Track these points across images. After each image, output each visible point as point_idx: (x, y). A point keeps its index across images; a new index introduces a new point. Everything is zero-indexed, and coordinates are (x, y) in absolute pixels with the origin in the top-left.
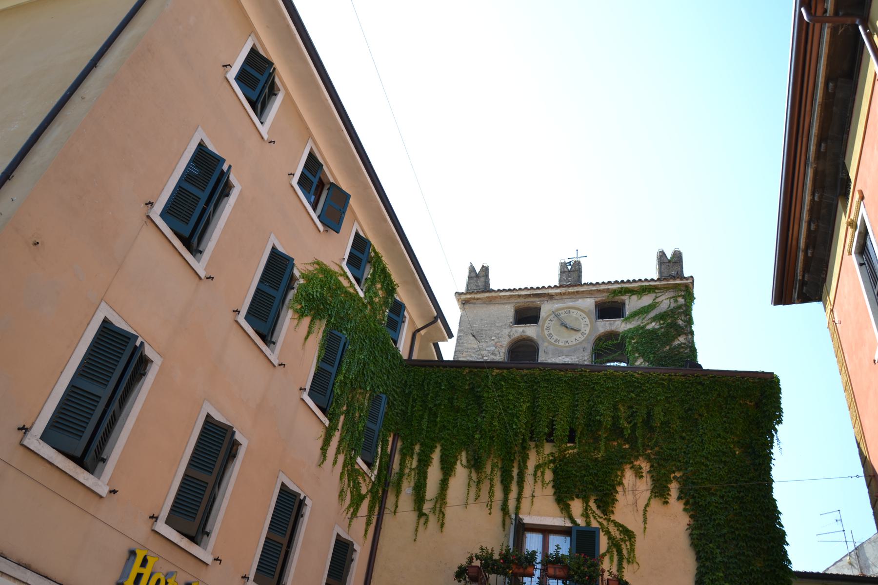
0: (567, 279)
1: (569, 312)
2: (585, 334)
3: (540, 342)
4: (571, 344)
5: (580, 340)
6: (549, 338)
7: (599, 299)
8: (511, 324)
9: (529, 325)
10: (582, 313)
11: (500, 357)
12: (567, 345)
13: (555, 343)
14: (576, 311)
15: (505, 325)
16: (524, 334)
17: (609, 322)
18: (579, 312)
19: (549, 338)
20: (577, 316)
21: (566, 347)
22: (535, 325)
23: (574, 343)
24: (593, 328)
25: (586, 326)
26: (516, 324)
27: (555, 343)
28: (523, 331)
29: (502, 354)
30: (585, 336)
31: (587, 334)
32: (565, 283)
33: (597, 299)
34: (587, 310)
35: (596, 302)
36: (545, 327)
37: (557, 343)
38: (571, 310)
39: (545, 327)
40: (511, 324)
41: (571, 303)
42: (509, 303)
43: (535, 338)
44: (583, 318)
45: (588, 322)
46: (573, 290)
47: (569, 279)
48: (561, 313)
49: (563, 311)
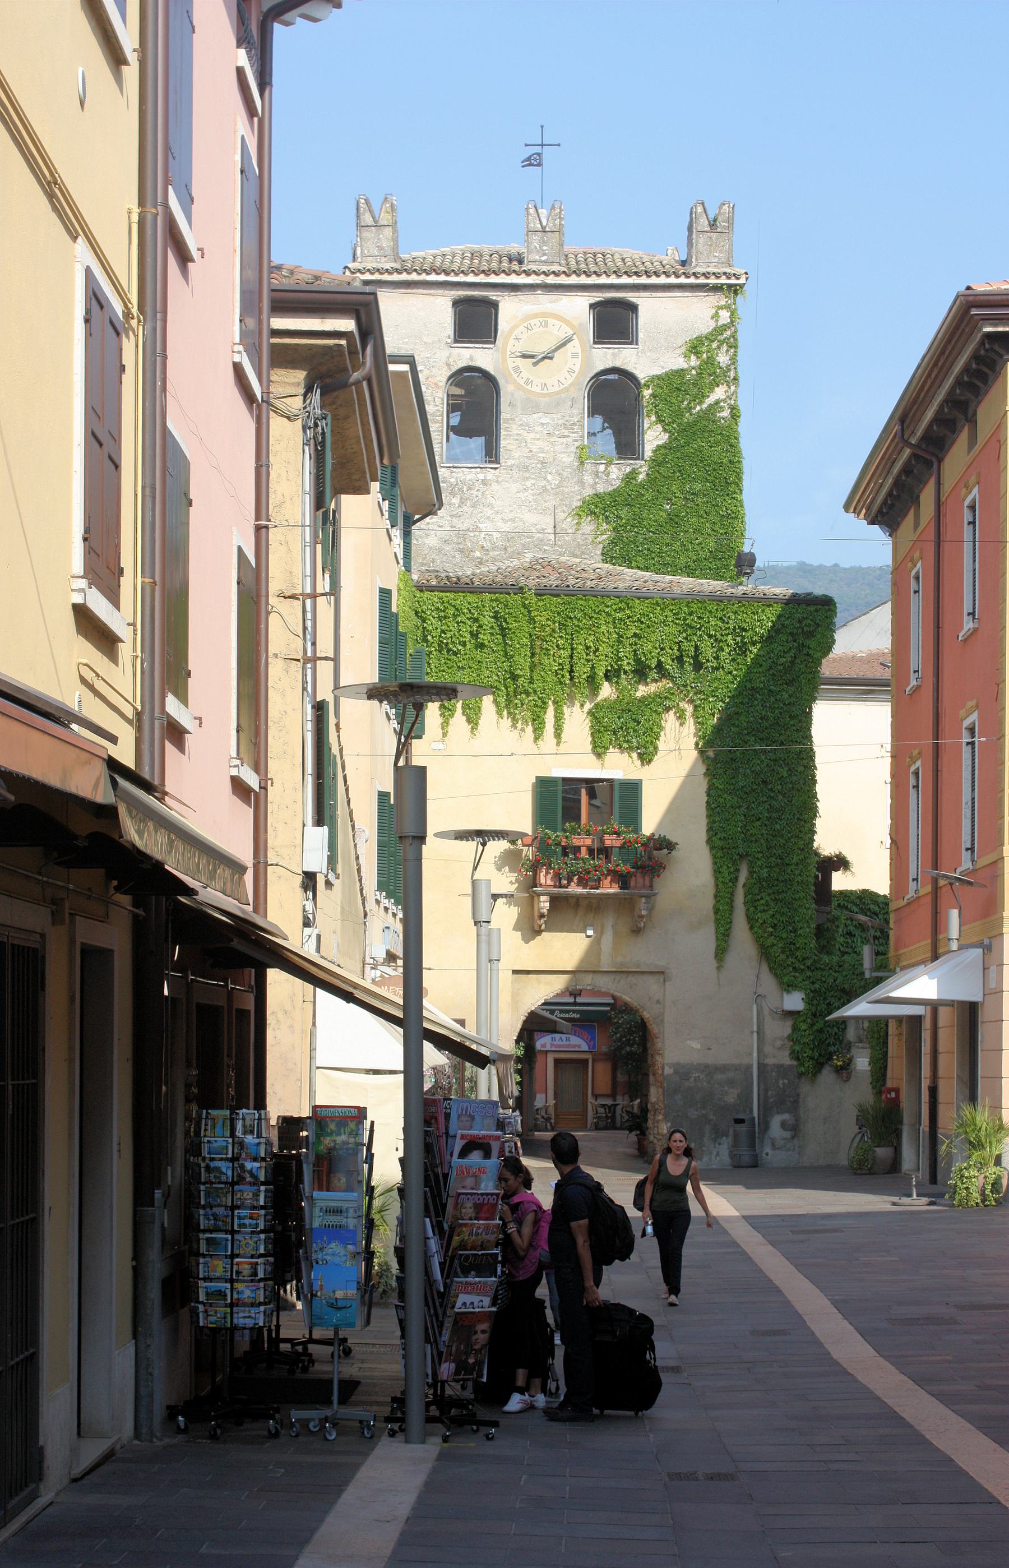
4: (551, 390)
8: (449, 341)
12: (545, 391)
13: (524, 385)
15: (439, 341)
21: (544, 395)
24: (587, 361)
27: (524, 385)
28: (471, 358)
32: (537, 257)
33: (592, 301)
36: (508, 353)
37: (529, 387)
39: (508, 353)
41: (549, 305)
47: (545, 248)
49: (536, 321)
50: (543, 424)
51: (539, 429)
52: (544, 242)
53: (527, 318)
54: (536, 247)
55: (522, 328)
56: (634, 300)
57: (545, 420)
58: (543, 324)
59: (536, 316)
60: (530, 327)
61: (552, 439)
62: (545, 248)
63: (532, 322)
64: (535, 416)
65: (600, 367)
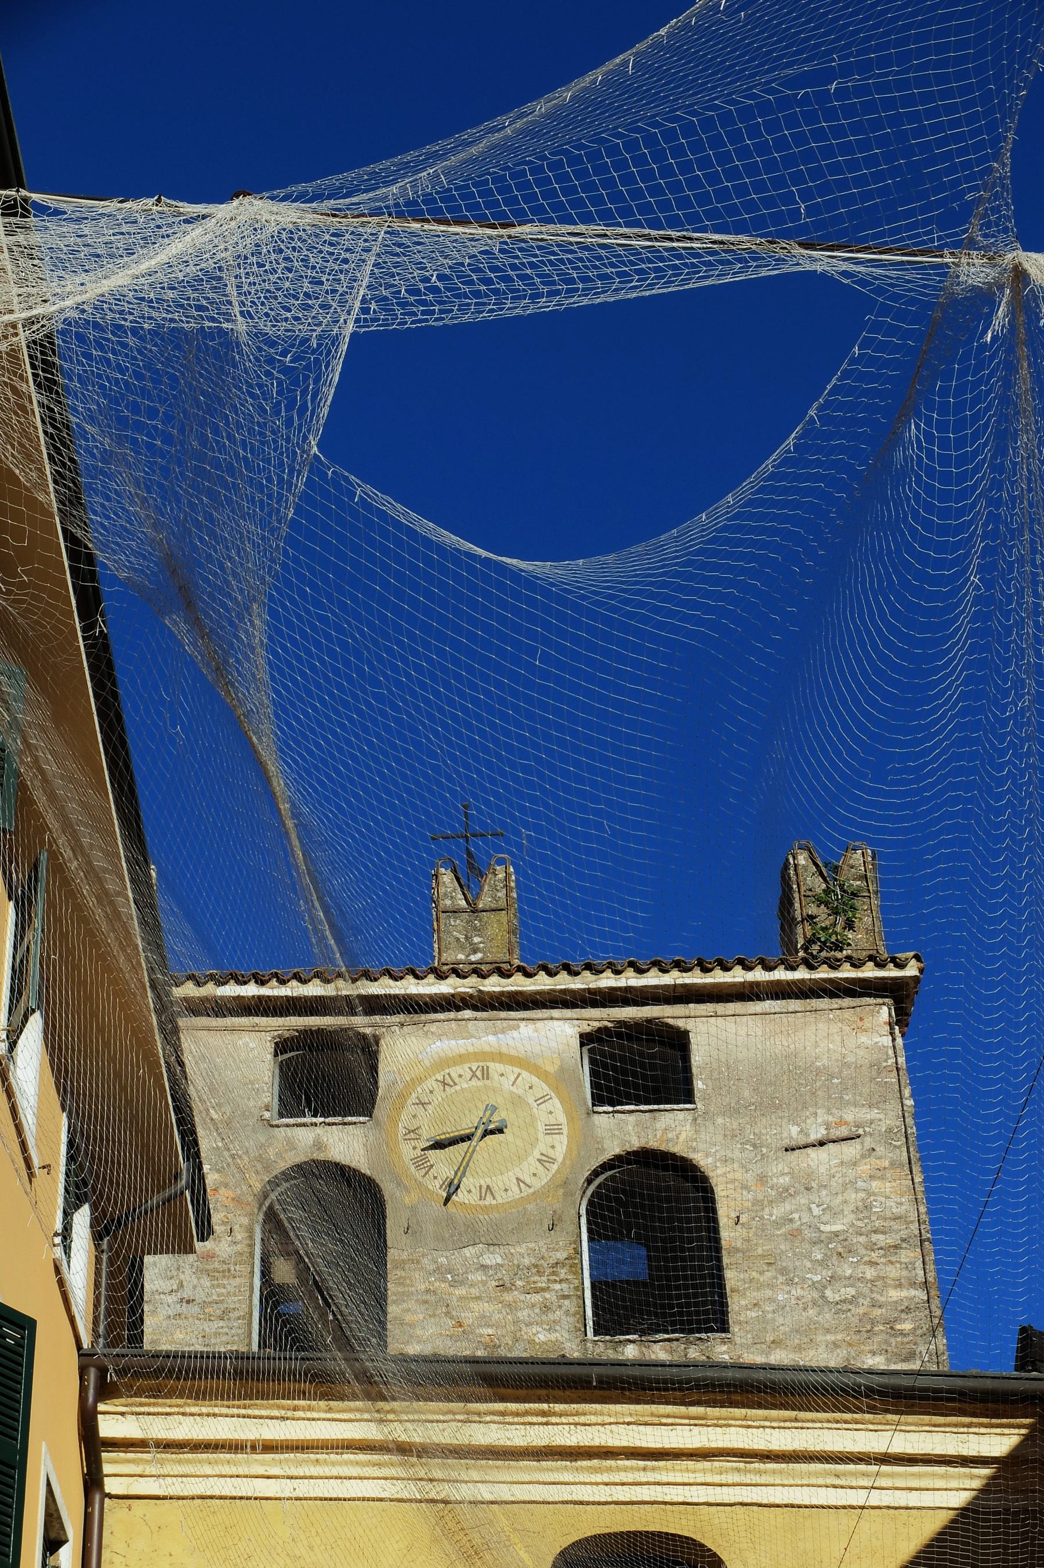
0: (467, 938)
1: (486, 1074)
2: (553, 1161)
3: (388, 1189)
4: (501, 1198)
5: (537, 1184)
6: (418, 1175)
7: (597, 1025)
9: (338, 1119)
10: (535, 1079)
11: (239, 1247)
12: (489, 1201)
14: (511, 1071)
16: (321, 1157)
17: (631, 1118)
18: (525, 1074)
19: (418, 1175)
20: (520, 1092)
21: (486, 1209)
22: (362, 1119)
23: (515, 1193)
24: (584, 1138)
25: (552, 1130)
26: (281, 1115)
28: (318, 1145)
29: (240, 1235)
30: (555, 1167)
31: (560, 1159)
32: (461, 957)
34: (551, 1069)
35: (585, 1039)
38: (495, 1067)
39: (402, 1131)
40: (267, 1115)
41: (491, 1038)
42: (255, 1029)
43: (365, 1170)
44: (542, 1100)
45: (562, 1118)
46: (497, 989)
47: (476, 940)
48: (454, 1075)
49: (464, 1069)
50: (484, 1267)
51: (479, 1276)
52: (475, 929)
53: (445, 1062)
54: (458, 939)
55: (431, 1083)
56: (681, 1023)
57: (493, 1258)
58: (479, 1073)
59: (461, 1059)
60: (448, 1080)
61: (508, 1297)
62: (476, 940)
63: (453, 1072)
64: (468, 1252)
65: (614, 1149)
